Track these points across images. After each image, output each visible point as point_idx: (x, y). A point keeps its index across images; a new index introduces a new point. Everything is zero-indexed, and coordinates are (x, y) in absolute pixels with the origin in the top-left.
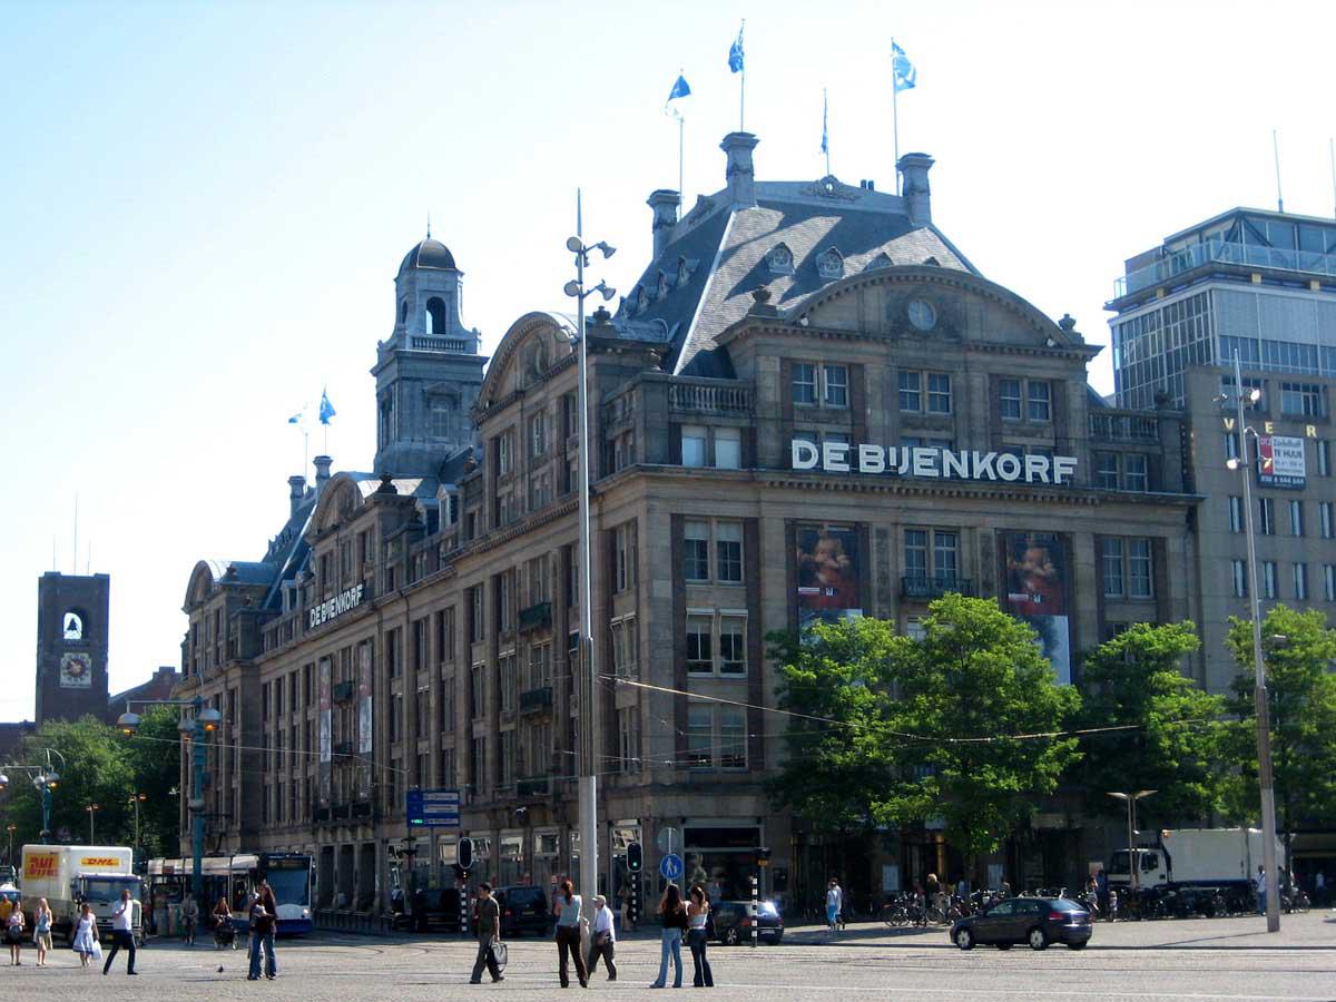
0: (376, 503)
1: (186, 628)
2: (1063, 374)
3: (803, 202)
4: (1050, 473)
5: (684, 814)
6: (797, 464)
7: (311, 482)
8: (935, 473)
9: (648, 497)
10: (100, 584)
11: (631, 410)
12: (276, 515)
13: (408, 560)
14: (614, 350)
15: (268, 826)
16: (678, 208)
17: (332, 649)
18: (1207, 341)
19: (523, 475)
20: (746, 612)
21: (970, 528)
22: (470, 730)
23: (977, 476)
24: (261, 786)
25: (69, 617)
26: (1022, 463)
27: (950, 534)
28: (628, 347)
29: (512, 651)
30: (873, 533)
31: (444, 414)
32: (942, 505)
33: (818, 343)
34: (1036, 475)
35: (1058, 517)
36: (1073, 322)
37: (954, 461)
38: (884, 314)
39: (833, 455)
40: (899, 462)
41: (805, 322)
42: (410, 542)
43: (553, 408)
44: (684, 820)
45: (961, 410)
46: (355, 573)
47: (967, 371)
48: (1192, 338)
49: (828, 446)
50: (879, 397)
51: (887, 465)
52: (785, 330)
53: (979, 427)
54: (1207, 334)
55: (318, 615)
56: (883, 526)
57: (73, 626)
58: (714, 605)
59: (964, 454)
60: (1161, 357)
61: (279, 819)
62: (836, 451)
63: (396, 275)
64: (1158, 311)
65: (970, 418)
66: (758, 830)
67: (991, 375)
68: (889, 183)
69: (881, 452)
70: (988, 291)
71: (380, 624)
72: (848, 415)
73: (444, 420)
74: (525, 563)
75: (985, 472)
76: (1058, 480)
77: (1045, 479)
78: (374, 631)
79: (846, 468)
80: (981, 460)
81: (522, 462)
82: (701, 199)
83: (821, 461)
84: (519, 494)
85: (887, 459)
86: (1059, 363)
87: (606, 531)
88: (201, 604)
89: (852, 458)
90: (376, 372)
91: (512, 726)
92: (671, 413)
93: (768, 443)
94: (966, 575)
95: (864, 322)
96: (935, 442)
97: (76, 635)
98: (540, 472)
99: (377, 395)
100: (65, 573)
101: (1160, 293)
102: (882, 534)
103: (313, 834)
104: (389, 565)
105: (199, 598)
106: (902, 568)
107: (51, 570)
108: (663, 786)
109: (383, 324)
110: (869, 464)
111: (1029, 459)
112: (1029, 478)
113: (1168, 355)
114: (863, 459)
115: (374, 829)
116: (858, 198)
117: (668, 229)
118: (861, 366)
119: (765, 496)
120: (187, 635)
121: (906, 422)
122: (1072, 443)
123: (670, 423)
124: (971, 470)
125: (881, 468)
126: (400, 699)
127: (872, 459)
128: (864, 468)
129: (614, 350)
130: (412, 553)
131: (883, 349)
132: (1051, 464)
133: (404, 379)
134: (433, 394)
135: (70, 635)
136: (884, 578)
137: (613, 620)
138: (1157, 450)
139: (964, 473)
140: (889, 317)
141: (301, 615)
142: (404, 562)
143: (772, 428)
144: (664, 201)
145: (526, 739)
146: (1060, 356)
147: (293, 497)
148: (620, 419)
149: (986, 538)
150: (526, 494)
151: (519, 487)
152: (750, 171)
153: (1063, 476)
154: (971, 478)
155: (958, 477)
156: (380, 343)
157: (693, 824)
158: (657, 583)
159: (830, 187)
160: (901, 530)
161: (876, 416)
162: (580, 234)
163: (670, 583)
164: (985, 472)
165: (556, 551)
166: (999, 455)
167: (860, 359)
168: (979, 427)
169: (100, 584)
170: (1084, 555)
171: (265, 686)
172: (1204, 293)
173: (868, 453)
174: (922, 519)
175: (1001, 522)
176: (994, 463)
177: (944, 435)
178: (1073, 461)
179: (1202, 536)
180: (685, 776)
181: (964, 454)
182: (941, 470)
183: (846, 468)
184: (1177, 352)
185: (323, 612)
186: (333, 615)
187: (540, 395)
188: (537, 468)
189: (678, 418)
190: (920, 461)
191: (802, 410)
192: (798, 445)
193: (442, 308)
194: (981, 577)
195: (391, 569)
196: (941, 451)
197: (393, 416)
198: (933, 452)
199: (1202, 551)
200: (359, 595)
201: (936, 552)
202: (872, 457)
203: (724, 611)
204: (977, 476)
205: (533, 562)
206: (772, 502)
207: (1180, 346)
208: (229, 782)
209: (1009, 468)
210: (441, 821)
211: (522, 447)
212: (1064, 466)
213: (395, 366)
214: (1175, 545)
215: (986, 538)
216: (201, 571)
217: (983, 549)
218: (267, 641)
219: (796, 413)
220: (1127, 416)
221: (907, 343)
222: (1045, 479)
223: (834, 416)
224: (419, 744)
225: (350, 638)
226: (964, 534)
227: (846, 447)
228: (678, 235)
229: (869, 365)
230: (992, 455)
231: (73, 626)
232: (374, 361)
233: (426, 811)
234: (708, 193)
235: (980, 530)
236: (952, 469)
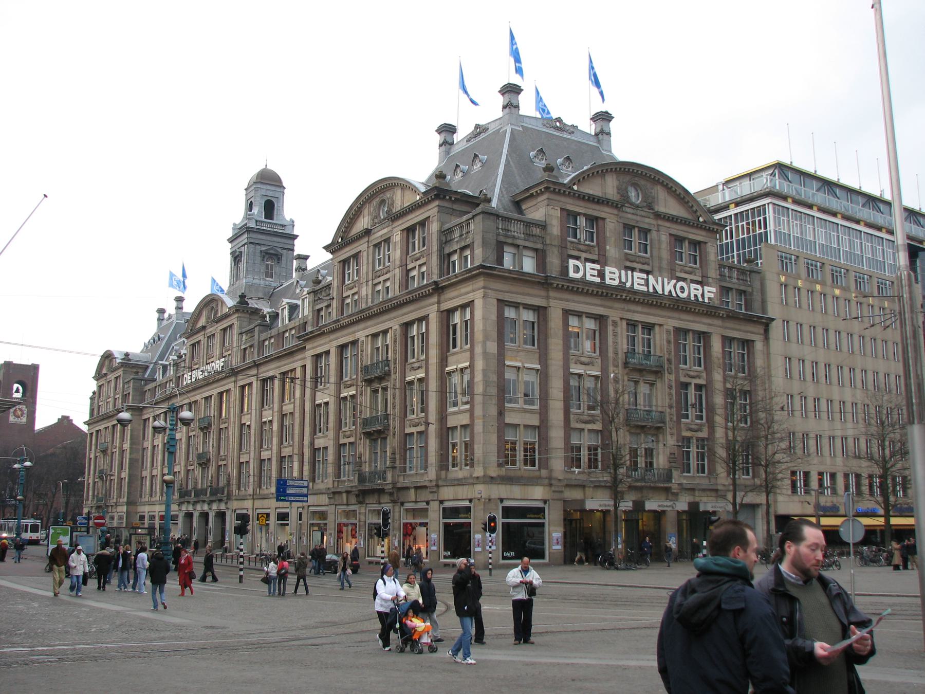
0: (237, 311)
1: (95, 388)
3: (544, 130)
4: (703, 295)
5: (502, 497)
6: (572, 274)
7: (171, 309)
8: (645, 289)
9: (484, 288)
10: (35, 368)
11: (468, 233)
12: (150, 329)
13: (259, 342)
14: (450, 198)
15: (143, 500)
16: (455, 136)
17: (198, 398)
18: (766, 233)
19: (367, 281)
20: (538, 367)
21: (660, 325)
22: (312, 444)
23: (666, 293)
24: (139, 477)
25: (16, 386)
27: (649, 328)
28: (459, 197)
29: (354, 392)
30: (610, 322)
31: (272, 266)
32: (646, 310)
33: (581, 203)
34: (696, 296)
35: (704, 324)
37: (655, 283)
38: (615, 191)
39: (590, 272)
40: (627, 280)
41: (575, 187)
42: (260, 332)
43: (397, 237)
44: (502, 500)
45: (655, 253)
46: (217, 352)
47: (658, 231)
48: (738, 235)
49: (589, 265)
50: (613, 239)
51: (620, 282)
52: (565, 191)
54: (765, 227)
55: (189, 378)
56: (615, 319)
57: (17, 391)
58: (520, 361)
59: (660, 279)
60: (732, 242)
61: (151, 496)
62: (594, 269)
63: (246, 187)
64: (730, 216)
65: (660, 259)
66: (544, 508)
67: (670, 235)
68: (588, 127)
69: (617, 274)
70: (670, 185)
71: (235, 382)
72: (596, 249)
73: (272, 269)
74: (367, 336)
75: (670, 292)
76: (706, 301)
78: (231, 386)
79: (598, 280)
80: (668, 283)
81: (367, 273)
82: (477, 126)
84: (363, 292)
85: (620, 277)
86: (704, 233)
87: (442, 312)
88: (105, 375)
89: (601, 274)
90: (231, 241)
91: (352, 440)
92: (498, 235)
93: (554, 261)
94: (658, 354)
95: (605, 193)
96: (642, 271)
97: (19, 395)
98: (382, 279)
99: (231, 254)
100: (17, 361)
101: (733, 205)
102: (615, 324)
103: (179, 505)
104: (243, 347)
105: (104, 371)
106: (625, 346)
107: (8, 360)
108: (492, 478)
109: (236, 214)
110: (610, 279)
111: (693, 286)
112: (692, 298)
113: (738, 241)
114: (608, 276)
115: (226, 503)
116: (573, 132)
117: (449, 147)
118: (604, 219)
119: (552, 294)
120: (94, 393)
121: (627, 257)
122: (710, 280)
123: (498, 241)
124: (663, 290)
125: (616, 283)
126: (249, 426)
127: (613, 276)
128: (608, 281)
129: (450, 198)
130: (262, 338)
131: (615, 212)
133: (251, 243)
134: (267, 253)
135: (15, 395)
136: (616, 353)
137: (447, 369)
138: (749, 289)
139: (660, 291)
140: (618, 193)
141: (174, 380)
142: (256, 344)
143: (556, 251)
144: (447, 130)
145: (364, 448)
146: (705, 229)
147: (159, 319)
148: (456, 240)
149: (668, 331)
150: (370, 292)
151: (364, 289)
152: (517, 107)
153: (709, 298)
154: (663, 294)
155: (657, 292)
156: (235, 224)
157: (507, 503)
158: (489, 344)
159: (558, 124)
160: (624, 323)
161: (612, 250)
162: (519, 71)
163: (496, 344)
164: (670, 292)
165: (397, 327)
166: (677, 282)
167: (603, 215)
168: (665, 264)
169: (35, 368)
170: (716, 346)
171: (145, 420)
172: (765, 205)
173: (610, 272)
174: (637, 317)
175: (677, 324)
176: (675, 287)
177: (646, 267)
178: (714, 290)
179: (771, 341)
180: (503, 471)
181: (660, 279)
182: (648, 288)
183: (598, 280)
184: (743, 239)
185: (193, 376)
186: (201, 377)
187: (385, 231)
188: (379, 277)
189: (502, 239)
190: (637, 280)
191: (571, 242)
192: (572, 262)
193: (270, 208)
194: (666, 356)
195: (245, 349)
196: (647, 276)
197: (243, 265)
198: (645, 276)
199: (772, 351)
200: (222, 364)
201: (643, 338)
202: (613, 276)
203: (527, 365)
204: (666, 293)
205: (375, 336)
206: (556, 299)
207: (745, 236)
208: (120, 473)
209: (682, 288)
210: (298, 498)
211: (368, 264)
212: (710, 292)
213: (246, 236)
214: (759, 346)
215: (668, 331)
216: (108, 357)
217: (667, 338)
218: (148, 395)
219: (569, 244)
221: (628, 210)
222: (700, 299)
223: (589, 249)
224: (262, 453)
225: (214, 391)
226: (657, 328)
227: (598, 267)
228: (456, 150)
229: (608, 220)
230: (674, 282)
231: (17, 391)
232: (230, 234)
233: (288, 492)
234: (482, 122)
235: (665, 327)
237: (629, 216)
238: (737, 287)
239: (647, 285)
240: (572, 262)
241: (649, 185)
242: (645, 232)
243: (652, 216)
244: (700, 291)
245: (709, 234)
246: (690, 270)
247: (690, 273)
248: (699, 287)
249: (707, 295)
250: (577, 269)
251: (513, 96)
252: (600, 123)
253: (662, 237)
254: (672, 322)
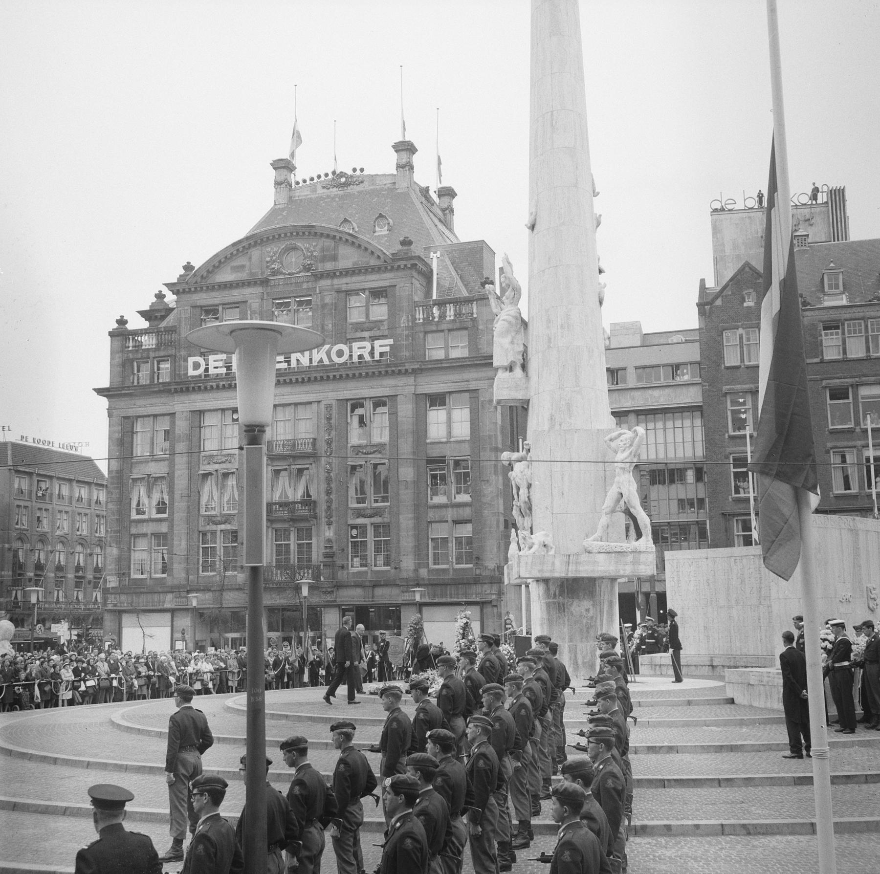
2: (393, 282)
4: (372, 353)
6: (191, 372)
21: (319, 402)
34: (360, 357)
36: (410, 243)
75: (321, 361)
76: (377, 357)
77: (367, 358)
80: (318, 352)
83: (207, 370)
111: (355, 345)
112: (355, 359)
119: (177, 398)
131: (259, 290)
132: (373, 348)
139: (305, 361)
149: (329, 407)
153: (381, 354)
164: (321, 361)
176: (328, 353)
178: (390, 341)
182: (289, 365)
189: (131, 356)
204: (315, 363)
209: (340, 353)
212: (382, 346)
215: (329, 407)
220: (450, 303)
222: (367, 358)
229: (250, 301)
230: (327, 347)
235: (323, 403)
236: (298, 360)
238: (450, 326)
239: (289, 362)
240: (191, 360)
243: (313, 278)
244: (369, 348)
245: (399, 274)
246: (372, 325)
247: (370, 330)
248: (368, 345)
249: (378, 351)
250: (196, 366)
251: (285, 172)
252: (405, 156)
254: (331, 394)
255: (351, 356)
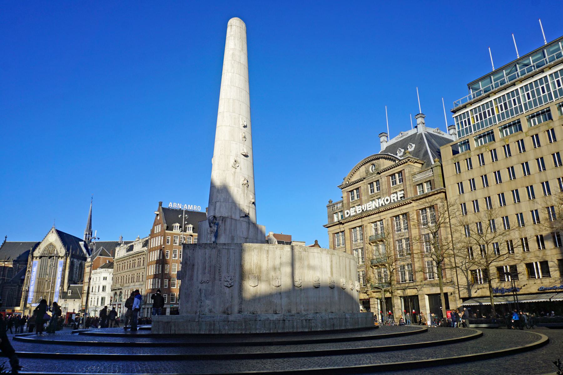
4: (397, 199)
26: (390, 198)
34: (394, 200)
38: (364, 172)
39: (352, 212)
53: (384, 192)
75: (382, 204)
76: (399, 199)
77: (396, 200)
86: (402, 166)
127: (359, 209)
161: (364, 198)
164: (382, 204)
177: (378, 197)
204: (380, 205)
209: (387, 200)
221: (369, 177)
222: (396, 200)
237: (370, 179)
241: (376, 161)
242: (377, 181)
244: (396, 197)
253: (384, 179)
255: (391, 201)
